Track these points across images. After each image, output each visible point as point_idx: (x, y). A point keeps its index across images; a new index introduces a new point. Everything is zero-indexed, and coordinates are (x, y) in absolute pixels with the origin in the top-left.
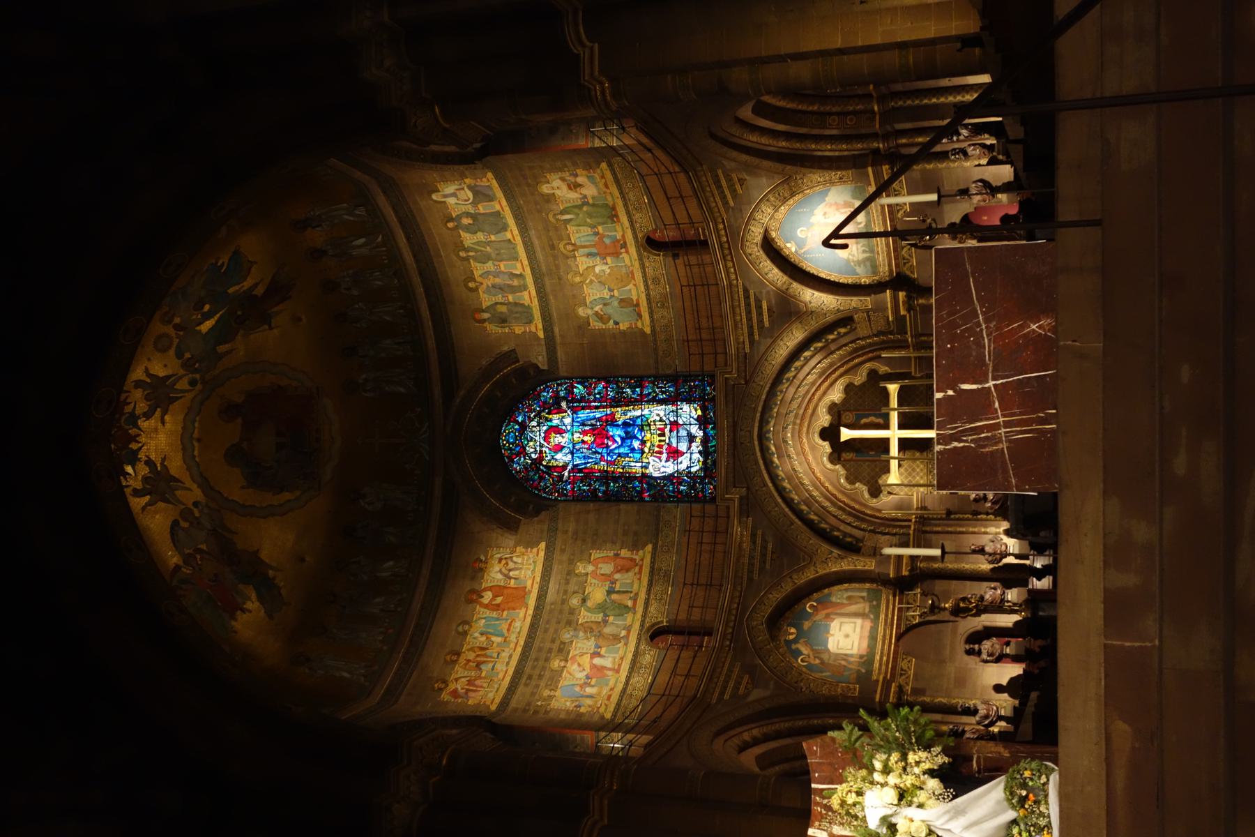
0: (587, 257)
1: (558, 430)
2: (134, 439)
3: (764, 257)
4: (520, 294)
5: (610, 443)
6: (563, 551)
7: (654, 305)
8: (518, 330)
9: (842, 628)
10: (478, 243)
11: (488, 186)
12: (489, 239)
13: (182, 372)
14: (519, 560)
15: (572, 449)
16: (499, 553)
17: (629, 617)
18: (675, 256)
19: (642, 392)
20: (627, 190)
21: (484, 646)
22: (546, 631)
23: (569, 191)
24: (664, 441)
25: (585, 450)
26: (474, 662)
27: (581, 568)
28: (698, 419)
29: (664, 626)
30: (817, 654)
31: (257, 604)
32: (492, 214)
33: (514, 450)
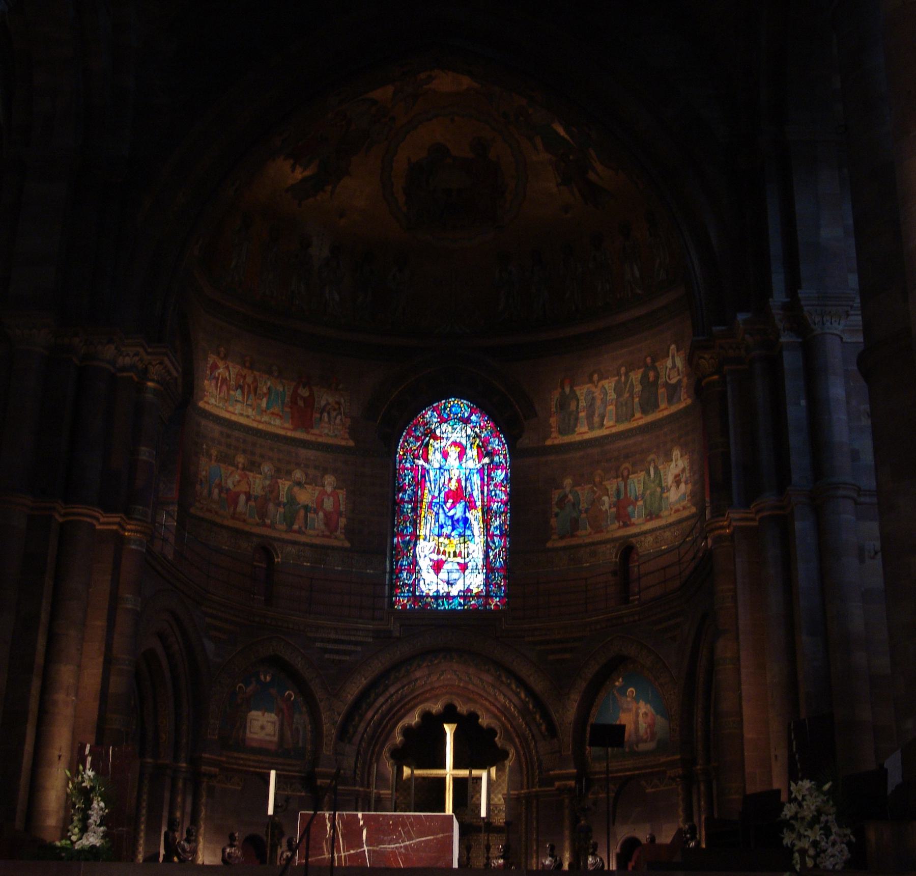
0: (616, 489)
1: (462, 454)
4: (586, 423)
5: (449, 505)
8: (553, 421)
9: (269, 724)
10: (632, 385)
11: (680, 399)
12: (635, 396)
14: (338, 421)
15: (445, 468)
16: (345, 401)
17: (283, 527)
19: (497, 536)
20: (673, 530)
21: (258, 391)
23: (673, 476)
24: (449, 556)
25: (442, 480)
26: (243, 382)
27: (329, 480)
28: (469, 590)
29: (274, 559)
31: (300, 177)
33: (444, 412)
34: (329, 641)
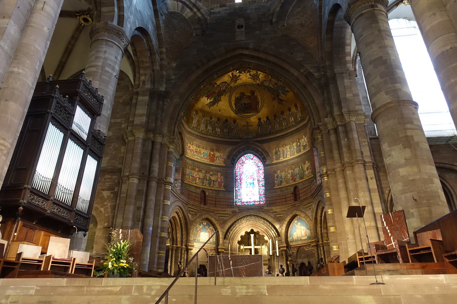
2: (245, 72)
3: (293, 215)
6: (223, 170)
7: (281, 189)
13: (260, 81)
14: (221, 160)
17: (208, 186)
18: (292, 193)
22: (205, 167)
27: (219, 174)
30: (200, 230)
32: (300, 149)
34: (220, 214)
